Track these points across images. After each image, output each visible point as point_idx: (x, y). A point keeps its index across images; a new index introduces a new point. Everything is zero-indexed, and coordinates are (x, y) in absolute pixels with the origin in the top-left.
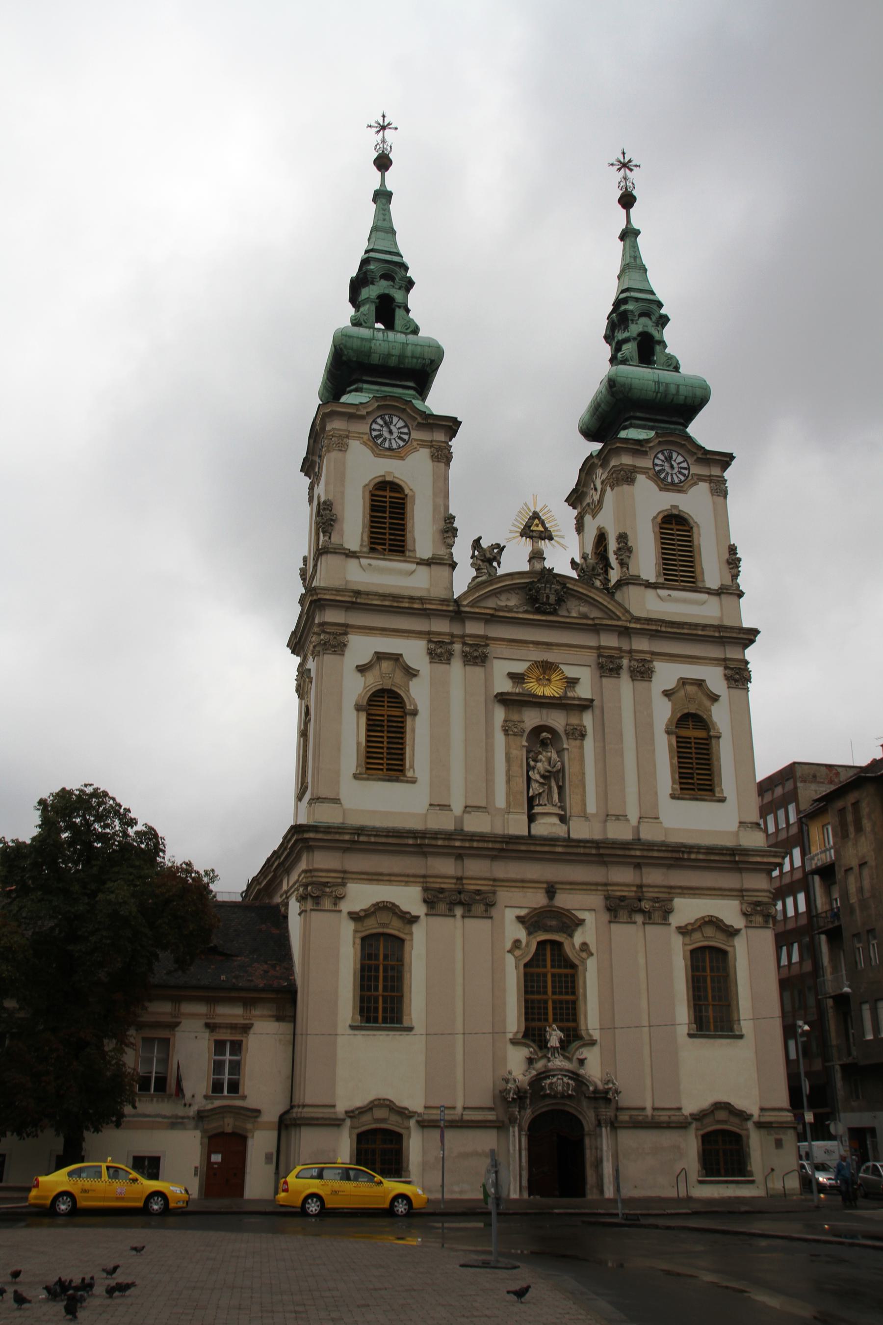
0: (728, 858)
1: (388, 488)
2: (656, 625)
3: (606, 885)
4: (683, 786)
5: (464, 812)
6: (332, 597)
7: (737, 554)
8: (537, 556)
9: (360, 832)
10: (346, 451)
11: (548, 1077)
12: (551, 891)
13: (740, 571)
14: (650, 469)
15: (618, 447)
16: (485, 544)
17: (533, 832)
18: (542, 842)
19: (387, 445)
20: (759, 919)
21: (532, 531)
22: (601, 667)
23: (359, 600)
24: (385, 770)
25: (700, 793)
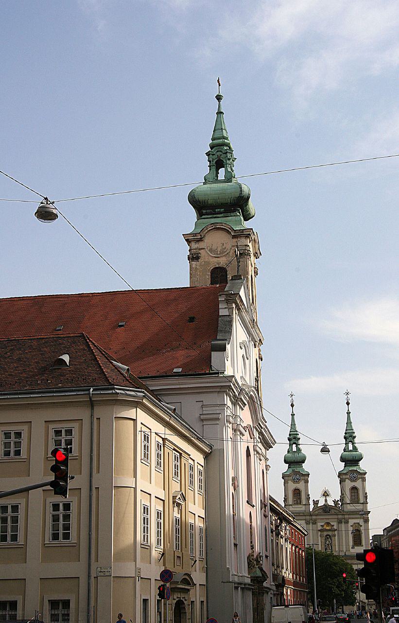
8: (326, 501)
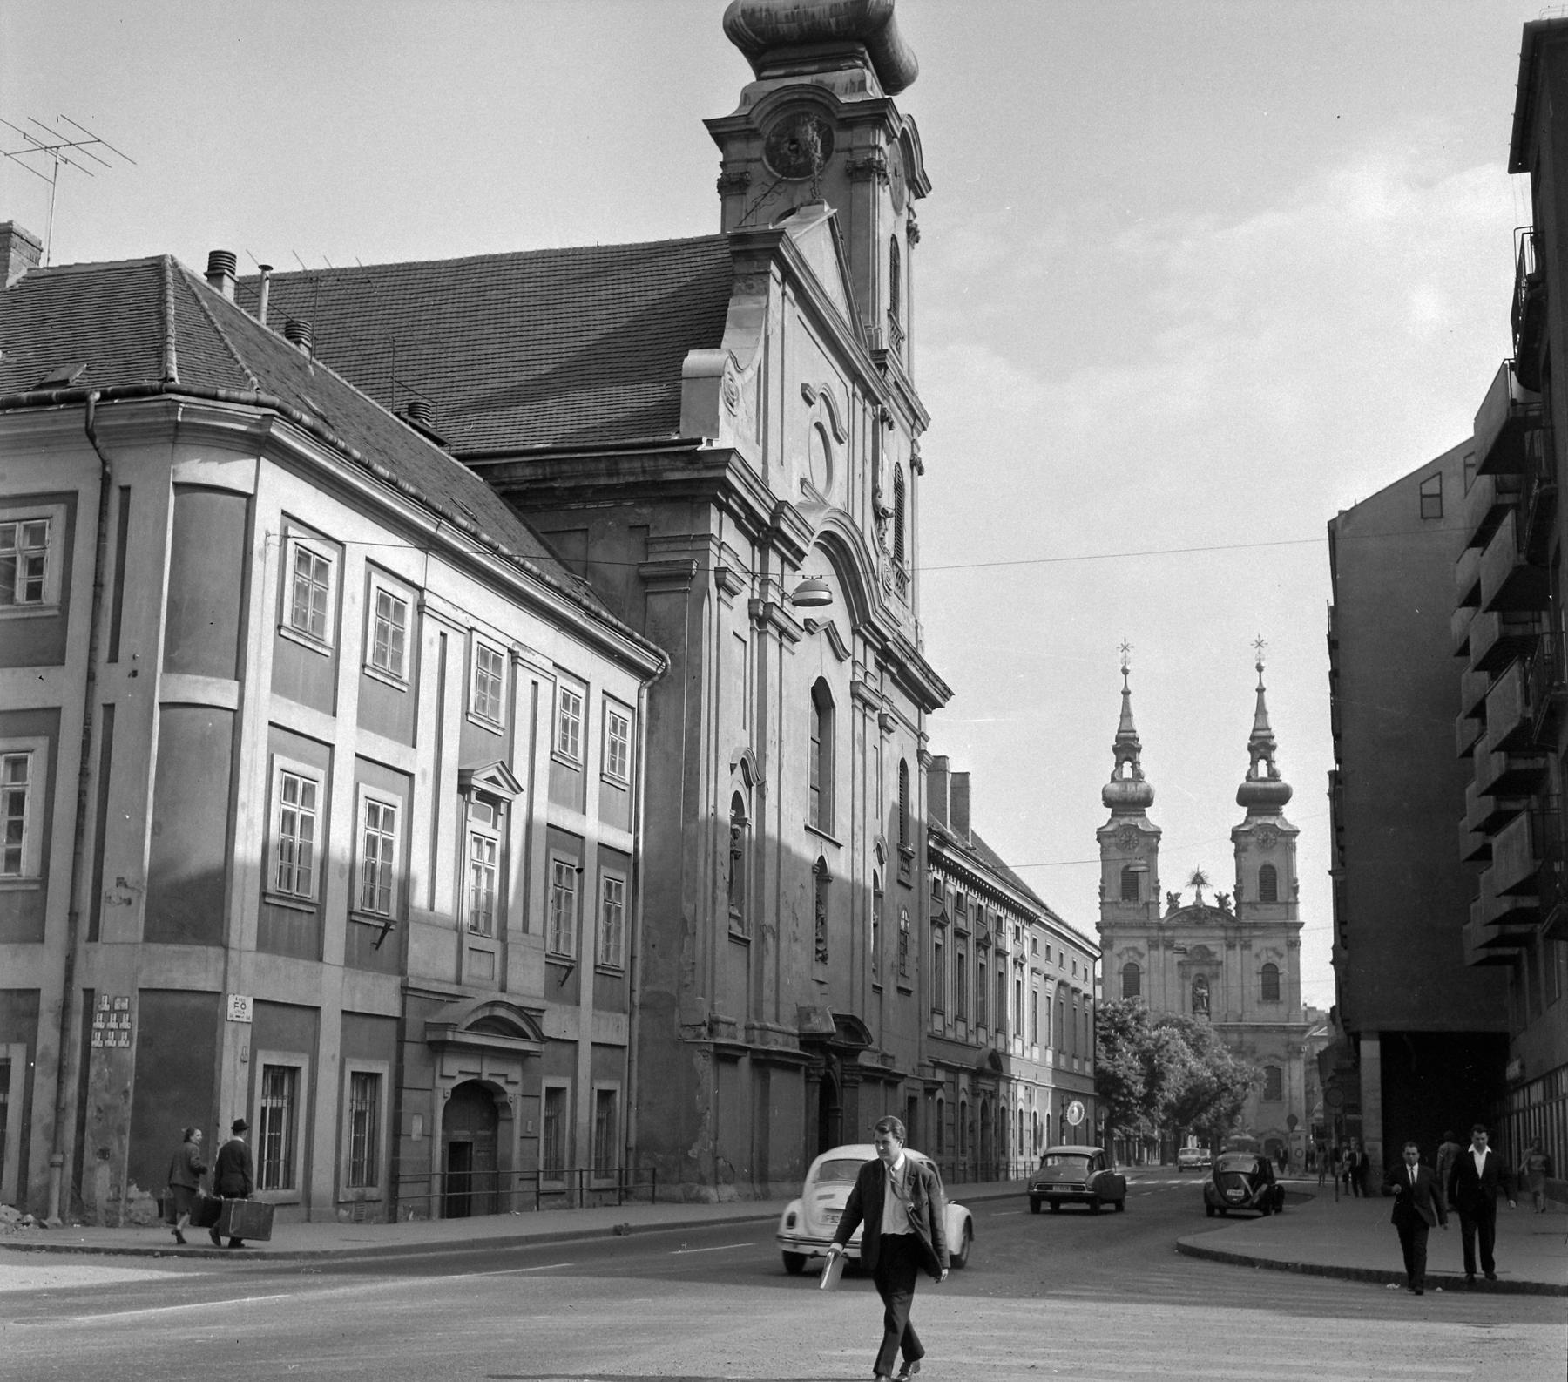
8: (1199, 895)
16: (1173, 893)
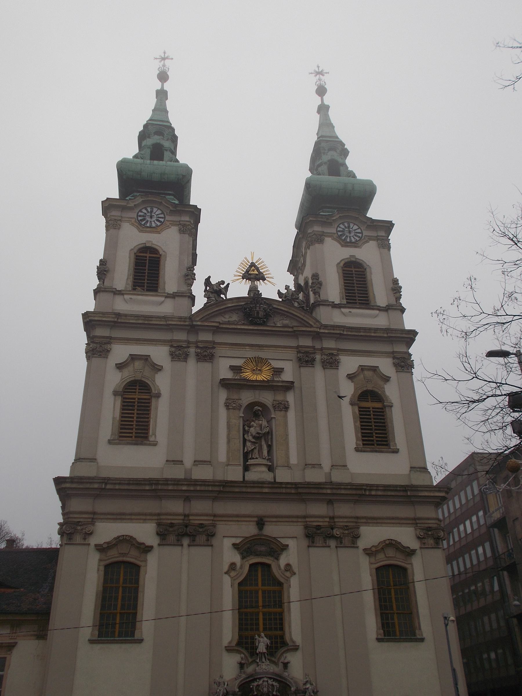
0: (401, 494)
1: (148, 251)
2: (339, 330)
3: (305, 517)
4: (365, 442)
5: (194, 465)
6: (100, 319)
7: (399, 284)
9: (106, 481)
10: (119, 229)
11: (255, 680)
12: (261, 523)
13: (401, 295)
14: (334, 233)
15: (311, 221)
16: (214, 281)
17: (247, 478)
18: (252, 485)
19: (148, 225)
20: (431, 542)
21: (250, 274)
22: (299, 360)
23: (119, 320)
24: (133, 437)
25: (378, 447)
